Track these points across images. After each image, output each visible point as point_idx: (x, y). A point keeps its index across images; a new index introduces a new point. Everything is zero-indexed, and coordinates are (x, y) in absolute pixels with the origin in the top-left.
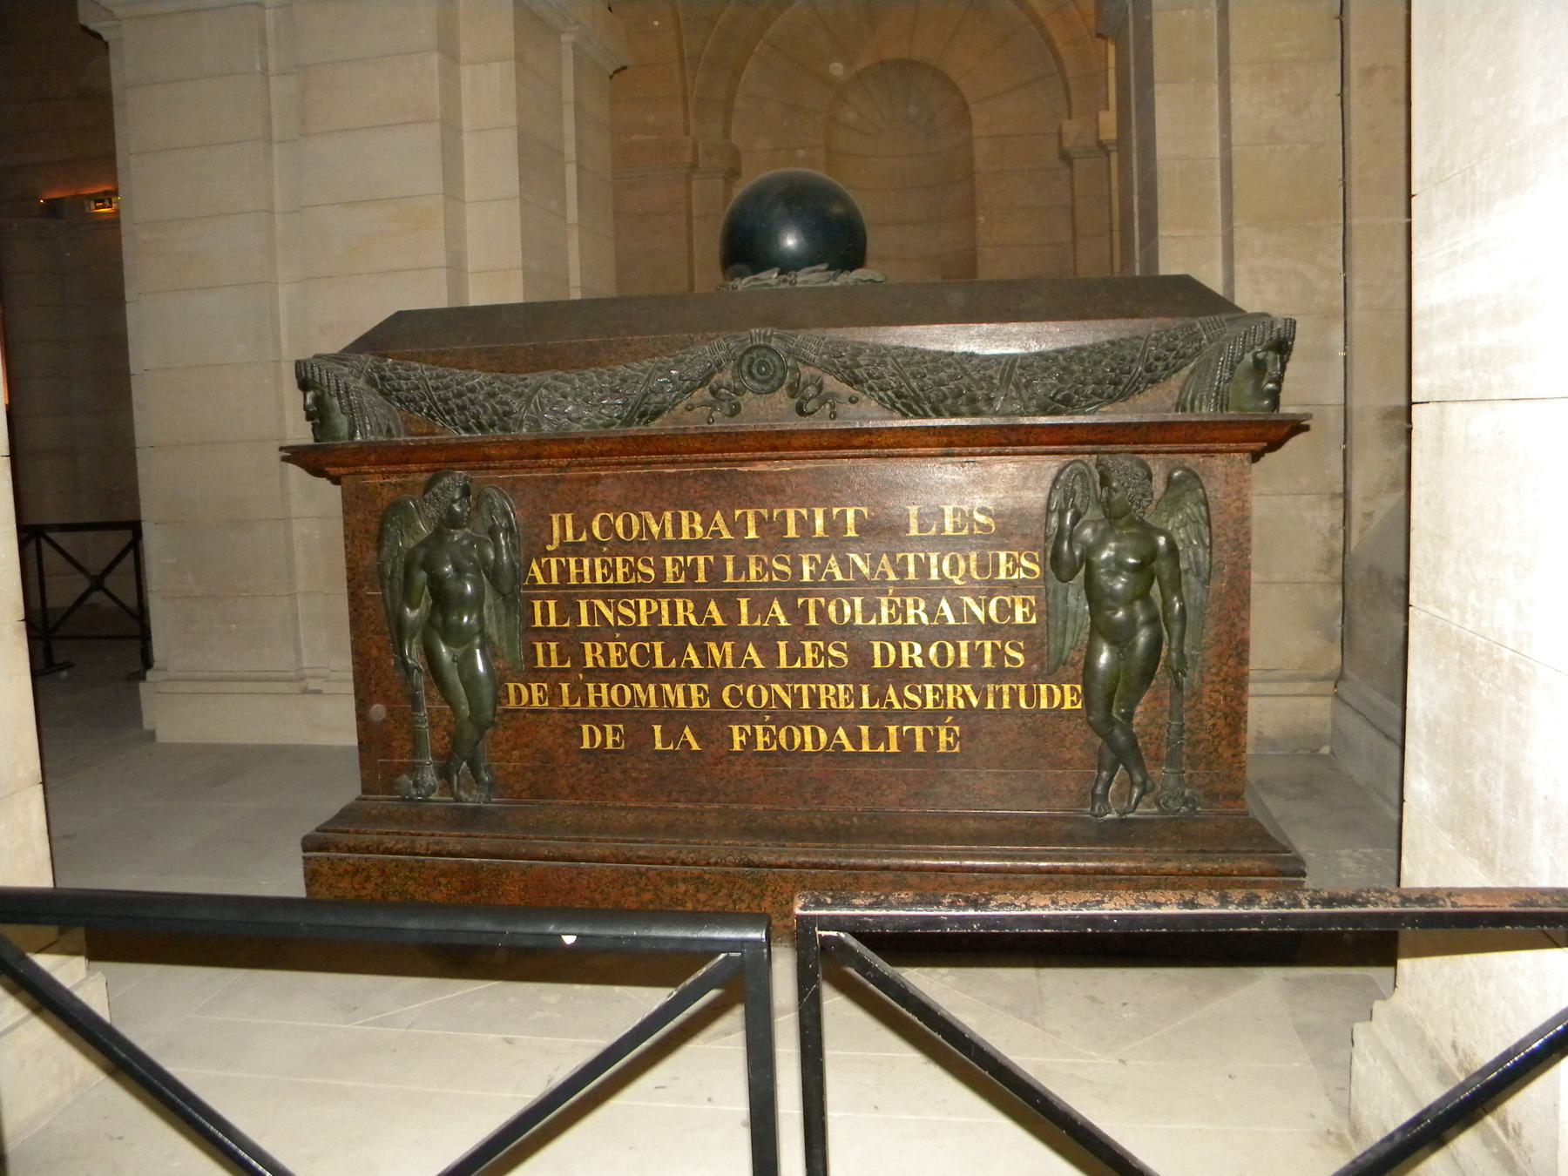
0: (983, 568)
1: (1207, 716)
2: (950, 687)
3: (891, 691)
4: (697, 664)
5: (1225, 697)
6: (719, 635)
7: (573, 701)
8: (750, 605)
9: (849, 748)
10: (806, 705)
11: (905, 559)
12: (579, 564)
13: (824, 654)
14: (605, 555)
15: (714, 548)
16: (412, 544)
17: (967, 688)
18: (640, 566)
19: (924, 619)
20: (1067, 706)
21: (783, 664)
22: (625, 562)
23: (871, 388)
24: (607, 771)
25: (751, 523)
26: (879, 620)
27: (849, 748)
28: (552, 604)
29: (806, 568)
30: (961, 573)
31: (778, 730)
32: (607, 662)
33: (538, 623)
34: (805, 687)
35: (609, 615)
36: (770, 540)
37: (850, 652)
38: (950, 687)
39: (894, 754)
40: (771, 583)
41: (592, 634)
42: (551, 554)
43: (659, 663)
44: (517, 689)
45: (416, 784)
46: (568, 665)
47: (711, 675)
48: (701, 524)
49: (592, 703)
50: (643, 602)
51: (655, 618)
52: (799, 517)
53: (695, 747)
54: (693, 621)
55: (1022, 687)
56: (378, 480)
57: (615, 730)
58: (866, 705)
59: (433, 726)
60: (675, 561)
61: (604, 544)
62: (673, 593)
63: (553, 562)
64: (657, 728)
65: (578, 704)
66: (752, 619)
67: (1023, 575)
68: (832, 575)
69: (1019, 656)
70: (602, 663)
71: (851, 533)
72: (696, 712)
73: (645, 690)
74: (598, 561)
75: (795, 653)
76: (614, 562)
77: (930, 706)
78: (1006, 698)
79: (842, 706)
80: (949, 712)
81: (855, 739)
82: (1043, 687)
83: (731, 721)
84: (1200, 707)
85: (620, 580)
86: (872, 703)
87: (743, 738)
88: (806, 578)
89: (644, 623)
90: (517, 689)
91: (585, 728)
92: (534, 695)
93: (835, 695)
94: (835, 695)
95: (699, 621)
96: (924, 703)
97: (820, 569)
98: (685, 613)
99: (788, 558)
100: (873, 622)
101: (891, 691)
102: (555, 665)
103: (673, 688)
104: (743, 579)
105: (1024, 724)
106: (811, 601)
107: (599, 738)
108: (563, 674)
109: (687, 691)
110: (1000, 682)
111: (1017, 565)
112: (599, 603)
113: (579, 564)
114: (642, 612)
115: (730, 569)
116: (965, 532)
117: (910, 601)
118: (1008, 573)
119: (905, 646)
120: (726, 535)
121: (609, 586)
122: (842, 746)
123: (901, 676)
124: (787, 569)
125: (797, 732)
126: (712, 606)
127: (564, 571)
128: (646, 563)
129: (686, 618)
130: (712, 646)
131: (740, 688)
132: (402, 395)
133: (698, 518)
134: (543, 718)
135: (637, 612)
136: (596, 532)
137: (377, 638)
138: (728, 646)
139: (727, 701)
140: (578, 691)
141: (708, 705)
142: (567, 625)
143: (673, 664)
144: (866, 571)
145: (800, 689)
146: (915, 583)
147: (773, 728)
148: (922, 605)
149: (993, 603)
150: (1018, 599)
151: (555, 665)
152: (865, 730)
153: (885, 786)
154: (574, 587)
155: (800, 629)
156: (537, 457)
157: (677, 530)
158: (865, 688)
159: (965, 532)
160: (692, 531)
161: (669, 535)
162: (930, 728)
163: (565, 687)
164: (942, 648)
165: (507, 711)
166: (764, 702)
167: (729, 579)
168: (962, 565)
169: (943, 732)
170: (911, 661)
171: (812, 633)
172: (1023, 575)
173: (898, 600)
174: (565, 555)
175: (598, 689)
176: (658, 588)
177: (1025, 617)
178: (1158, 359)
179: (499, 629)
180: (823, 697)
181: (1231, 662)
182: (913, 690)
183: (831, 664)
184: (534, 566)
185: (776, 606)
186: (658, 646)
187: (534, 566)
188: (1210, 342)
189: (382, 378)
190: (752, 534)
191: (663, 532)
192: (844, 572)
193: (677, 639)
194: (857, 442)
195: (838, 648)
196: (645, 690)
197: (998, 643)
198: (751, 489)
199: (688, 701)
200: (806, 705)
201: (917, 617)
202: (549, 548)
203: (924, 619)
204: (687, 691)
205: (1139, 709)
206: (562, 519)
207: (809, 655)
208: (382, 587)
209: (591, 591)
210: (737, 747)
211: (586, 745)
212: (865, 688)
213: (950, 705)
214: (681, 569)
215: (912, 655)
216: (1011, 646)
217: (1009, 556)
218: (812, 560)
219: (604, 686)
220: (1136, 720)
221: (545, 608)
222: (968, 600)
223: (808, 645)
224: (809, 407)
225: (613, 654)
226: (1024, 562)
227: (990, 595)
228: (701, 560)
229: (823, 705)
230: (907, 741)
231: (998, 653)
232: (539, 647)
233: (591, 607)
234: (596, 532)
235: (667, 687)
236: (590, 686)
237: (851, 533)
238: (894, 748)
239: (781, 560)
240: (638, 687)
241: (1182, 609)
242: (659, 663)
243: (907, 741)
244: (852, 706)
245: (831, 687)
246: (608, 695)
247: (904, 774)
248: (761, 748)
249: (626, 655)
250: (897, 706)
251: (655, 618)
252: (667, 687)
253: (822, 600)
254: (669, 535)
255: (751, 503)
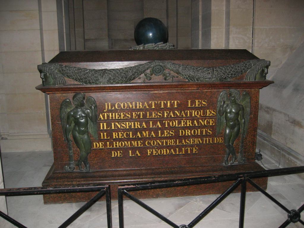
0: (203, 114)
1: (248, 143)
2: (196, 139)
3: (183, 141)
4: (140, 136)
5: (252, 139)
6: (145, 130)
7: (110, 146)
8: (152, 123)
9: (174, 153)
10: (165, 144)
11: (187, 112)
12: (112, 115)
13: (169, 133)
14: (119, 112)
15: (144, 110)
16: (69, 110)
17: (200, 139)
18: (127, 115)
19: (191, 125)
20: (220, 142)
21: (160, 136)
22: (123, 114)
23: (182, 75)
24: (118, 162)
25: (153, 104)
26: (181, 125)
27: (174, 153)
28: (105, 124)
29: (166, 114)
30: (199, 115)
31: (158, 150)
32: (119, 137)
33: (102, 128)
34: (164, 141)
35: (119, 126)
36: (157, 108)
37: (175, 132)
38: (196, 139)
39: (184, 154)
40: (157, 118)
41: (114, 131)
42: (105, 112)
43: (131, 137)
44: (96, 144)
45: (70, 168)
46: (109, 138)
47: (143, 139)
48: (142, 105)
49: (115, 146)
50: (127, 123)
51: (130, 126)
52: (164, 103)
53: (139, 155)
54: (139, 127)
55: (211, 139)
56: (60, 95)
57: (120, 152)
58: (178, 144)
59: (74, 154)
60: (135, 113)
61: (118, 110)
62: (135, 121)
63: (106, 114)
64: (130, 151)
65: (111, 147)
66: (153, 126)
67: (212, 115)
68: (171, 116)
69: (211, 132)
70: (117, 137)
71: (176, 106)
72: (139, 147)
73: (128, 143)
74: (117, 114)
75: (162, 133)
76: (121, 114)
77: (191, 143)
78: (208, 141)
79: (172, 144)
80: (196, 145)
81: (175, 151)
82: (215, 138)
83: (147, 149)
84: (247, 141)
85: (122, 118)
86: (179, 143)
87: (150, 152)
88: (165, 116)
89: (128, 128)
90: (96, 144)
91: (113, 152)
92: (100, 145)
93: (171, 142)
94: (171, 142)
95: (141, 127)
96: (190, 143)
97: (168, 114)
98: (138, 125)
99: (161, 112)
100: (180, 126)
101: (183, 141)
102: (106, 138)
103: (134, 142)
104: (151, 117)
105: (211, 146)
106: (166, 122)
107: (116, 154)
108: (108, 140)
109: (137, 143)
110: (206, 138)
111: (211, 113)
112: (117, 123)
113: (112, 115)
114: (127, 125)
115: (148, 115)
116: (200, 106)
117: (188, 121)
118: (209, 114)
119: (187, 131)
120: (147, 107)
121: (119, 119)
122: (172, 153)
123: (185, 137)
124: (161, 115)
125: (162, 151)
126: (144, 123)
127: (108, 116)
128: (128, 114)
129: (138, 126)
130: (144, 132)
131: (150, 141)
132: (69, 75)
133: (141, 103)
134: (103, 150)
135: (126, 125)
136: (116, 107)
137: (59, 133)
138: (147, 132)
139: (147, 144)
140: (112, 144)
141: (142, 146)
142: (109, 129)
143: (134, 137)
144: (179, 115)
145: (163, 141)
146: (189, 117)
147: (157, 150)
148: (191, 122)
149: (206, 121)
150: (211, 120)
151: (106, 138)
152: (177, 149)
153: (181, 161)
154: (111, 120)
155: (163, 128)
156: (104, 90)
157: (136, 107)
158: (178, 140)
159: (200, 106)
160: (140, 107)
161: (134, 108)
162: (191, 148)
163: (108, 143)
164: (195, 131)
165: (93, 149)
166: (155, 144)
167: (148, 117)
168: (199, 113)
169: (194, 149)
170: (188, 134)
171: (166, 129)
172: (212, 115)
173: (185, 121)
174: (109, 112)
175: (116, 143)
176: (131, 120)
177: (212, 124)
178: (243, 69)
179: (92, 130)
180: (168, 142)
181: (253, 132)
182: (188, 140)
183: (170, 135)
184: (101, 115)
185: (158, 123)
186: (131, 133)
187: (101, 115)
188: (253, 65)
189: (63, 70)
190: (153, 107)
191: (132, 107)
192: (174, 115)
193: (135, 131)
194: (179, 87)
195: (172, 132)
196: (128, 143)
197: (206, 129)
198: (153, 97)
199: (138, 145)
200: (165, 144)
201: (189, 124)
202: (105, 111)
203: (191, 125)
204: (137, 143)
205: (235, 142)
206: (108, 104)
207: (166, 133)
208: (61, 121)
209: (115, 121)
210: (149, 155)
211: (113, 156)
212: (178, 140)
213: (196, 143)
214: (136, 115)
215: (188, 133)
216: (209, 130)
217: (209, 111)
218: (167, 112)
219: (118, 142)
220: (234, 144)
221: (103, 125)
222: (200, 120)
223: (165, 131)
224: (167, 79)
225: (120, 135)
226: (212, 112)
227: (205, 119)
228: (141, 113)
229: (168, 144)
230: (186, 151)
231: (206, 132)
232: (102, 134)
233: (115, 125)
234: (116, 107)
235: (133, 142)
236: (114, 143)
237: (176, 106)
238: (183, 153)
239: (160, 113)
240: (126, 142)
241: (245, 121)
242: (131, 137)
243: (186, 151)
244: (175, 144)
245: (170, 140)
246: (119, 144)
247: (186, 158)
248: (154, 154)
249: (123, 135)
250: (184, 144)
251: (130, 126)
252: (133, 142)
253: (169, 121)
254: (134, 108)
255: (153, 100)
